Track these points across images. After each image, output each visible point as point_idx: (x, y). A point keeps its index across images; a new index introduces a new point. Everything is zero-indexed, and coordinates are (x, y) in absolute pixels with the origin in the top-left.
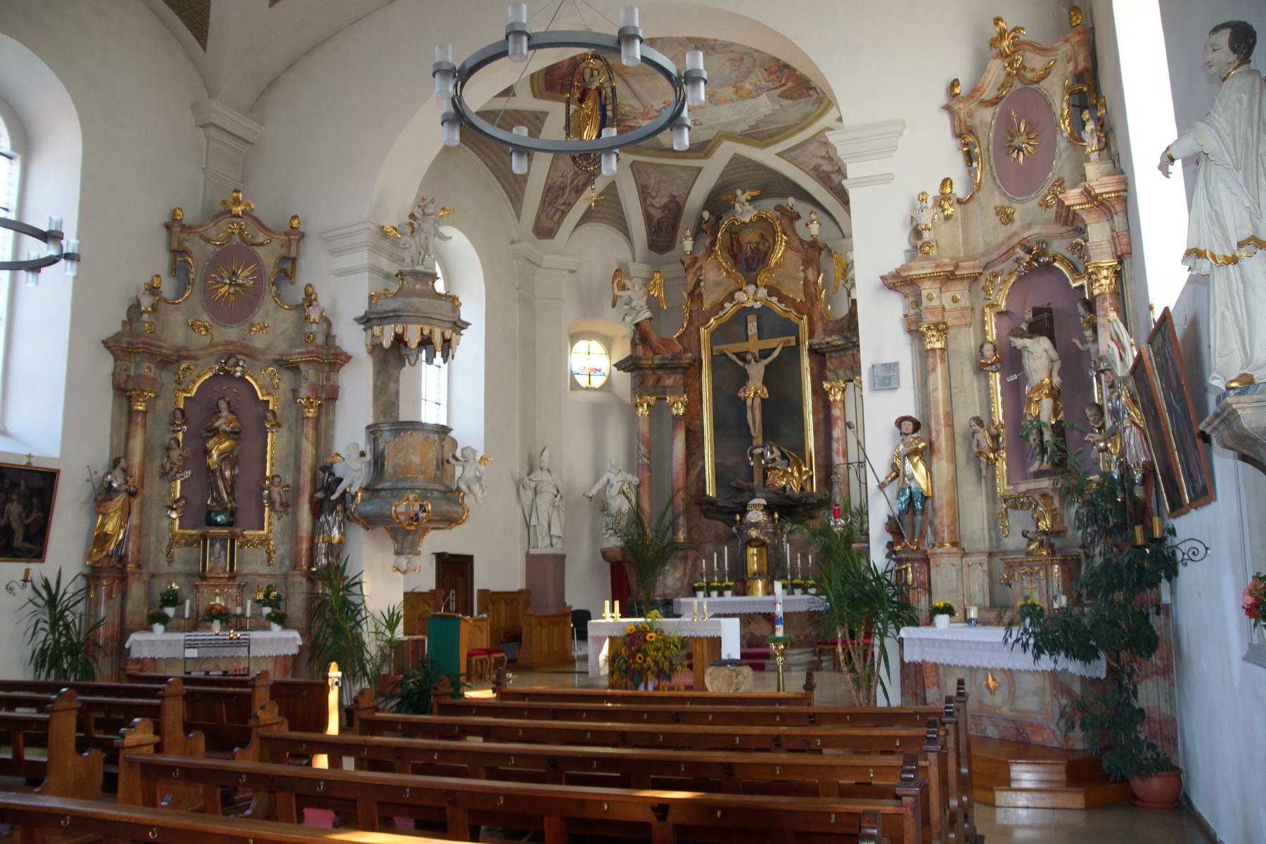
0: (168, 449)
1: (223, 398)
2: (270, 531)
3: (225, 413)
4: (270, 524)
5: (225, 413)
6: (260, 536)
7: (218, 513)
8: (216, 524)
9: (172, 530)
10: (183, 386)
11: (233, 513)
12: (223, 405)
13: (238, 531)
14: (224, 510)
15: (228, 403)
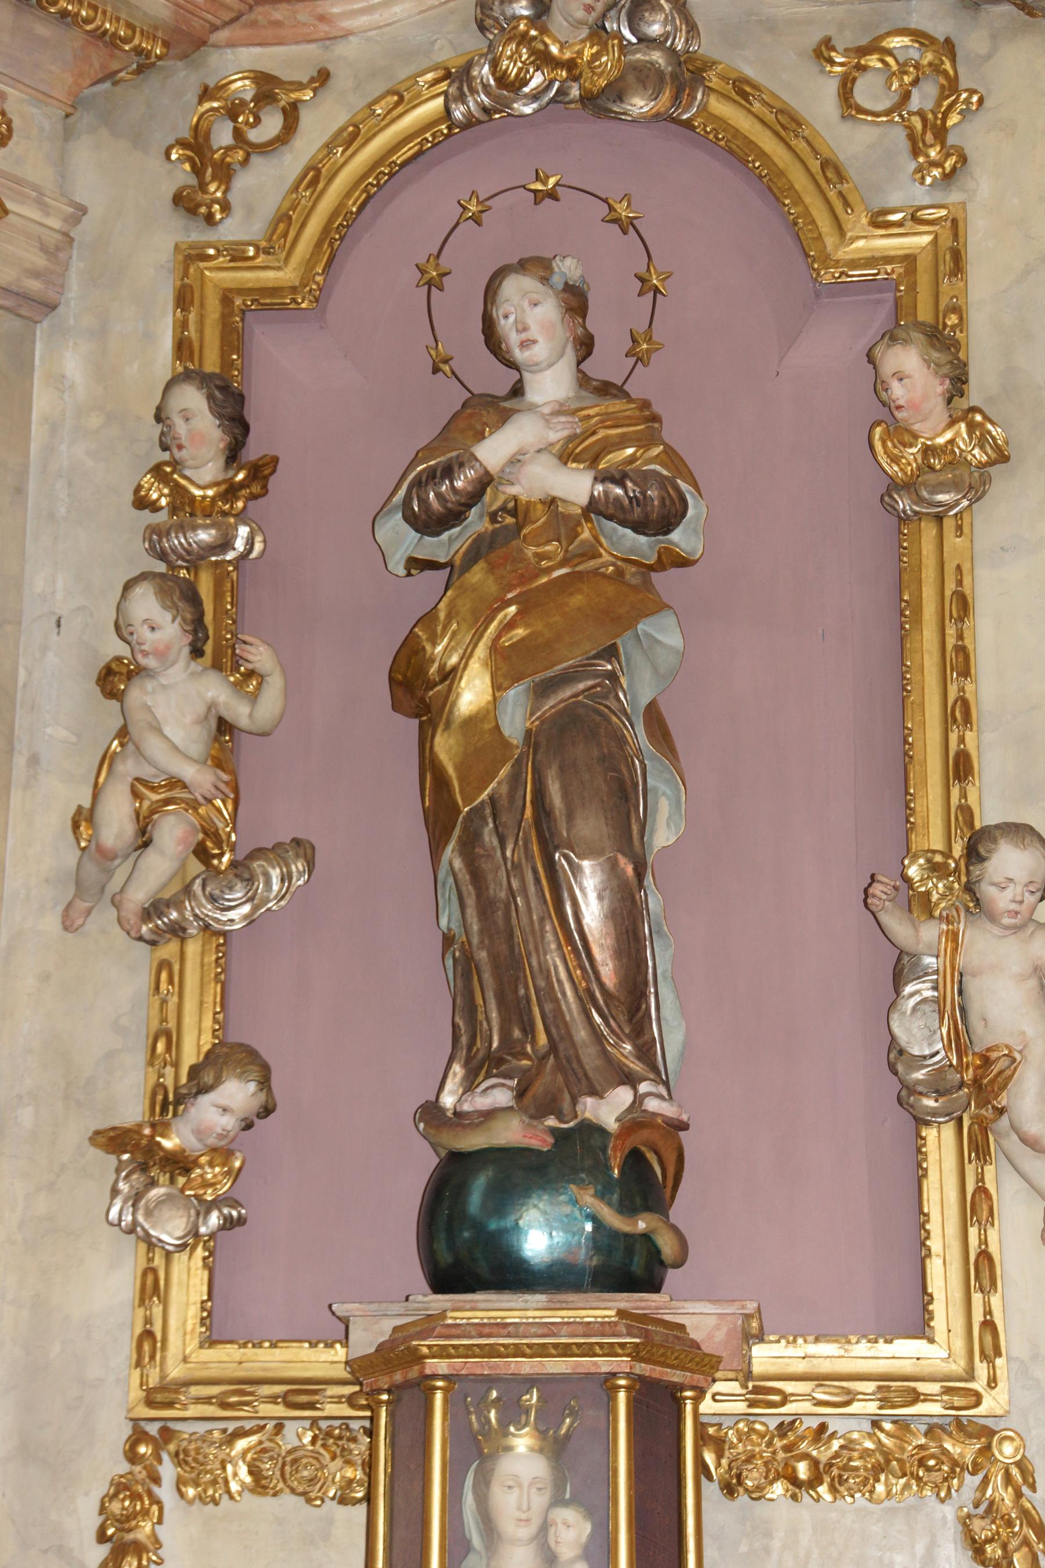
0: (114, 680)
1: (538, 266)
2: (987, 1342)
3: (551, 384)
4: (982, 1271)
5: (551, 384)
6: (898, 1389)
7: (522, 1173)
8: (512, 1275)
9: (149, 1342)
10: (231, 229)
11: (643, 1172)
12: (532, 316)
13: (702, 1319)
14: (574, 1155)
15: (576, 301)
